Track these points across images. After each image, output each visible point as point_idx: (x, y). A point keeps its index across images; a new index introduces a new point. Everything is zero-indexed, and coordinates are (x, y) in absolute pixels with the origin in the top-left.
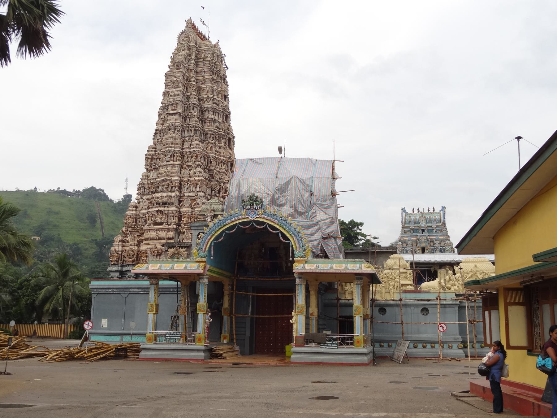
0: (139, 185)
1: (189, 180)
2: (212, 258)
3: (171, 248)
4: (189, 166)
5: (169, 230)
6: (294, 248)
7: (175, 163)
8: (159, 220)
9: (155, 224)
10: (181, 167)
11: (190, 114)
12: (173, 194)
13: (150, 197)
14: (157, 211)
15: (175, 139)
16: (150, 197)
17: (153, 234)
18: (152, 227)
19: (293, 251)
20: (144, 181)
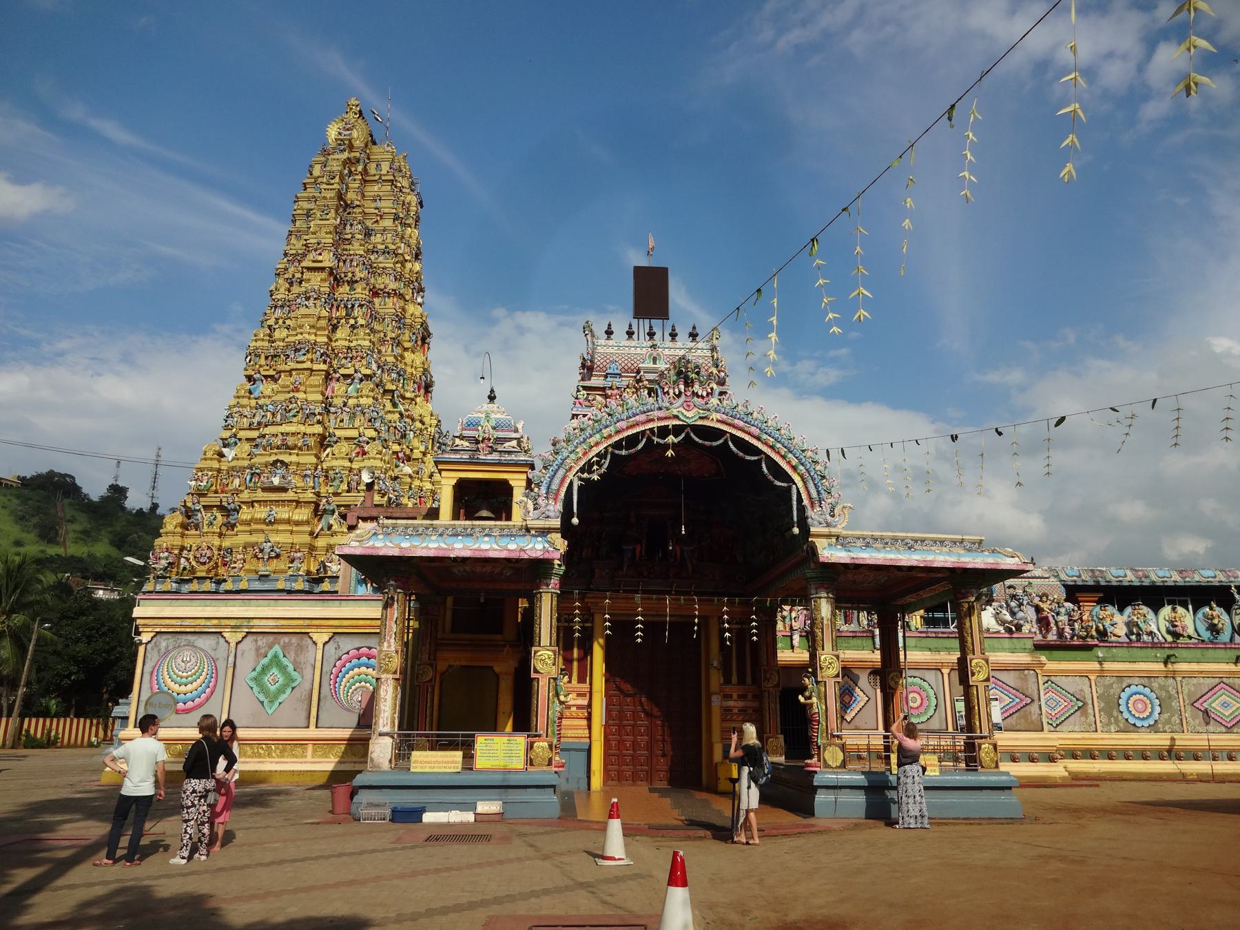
0: (230, 408)
1: (345, 404)
2: (575, 521)
3: (365, 519)
4: (346, 376)
5: (298, 503)
6: (806, 502)
7: (315, 367)
8: (276, 481)
9: (264, 490)
10: (328, 377)
11: (350, 275)
12: (310, 430)
13: (255, 434)
14: (275, 463)
15: (319, 318)
16: (255, 434)
17: (261, 512)
18: (260, 495)
19: (801, 509)
20: (244, 401)
